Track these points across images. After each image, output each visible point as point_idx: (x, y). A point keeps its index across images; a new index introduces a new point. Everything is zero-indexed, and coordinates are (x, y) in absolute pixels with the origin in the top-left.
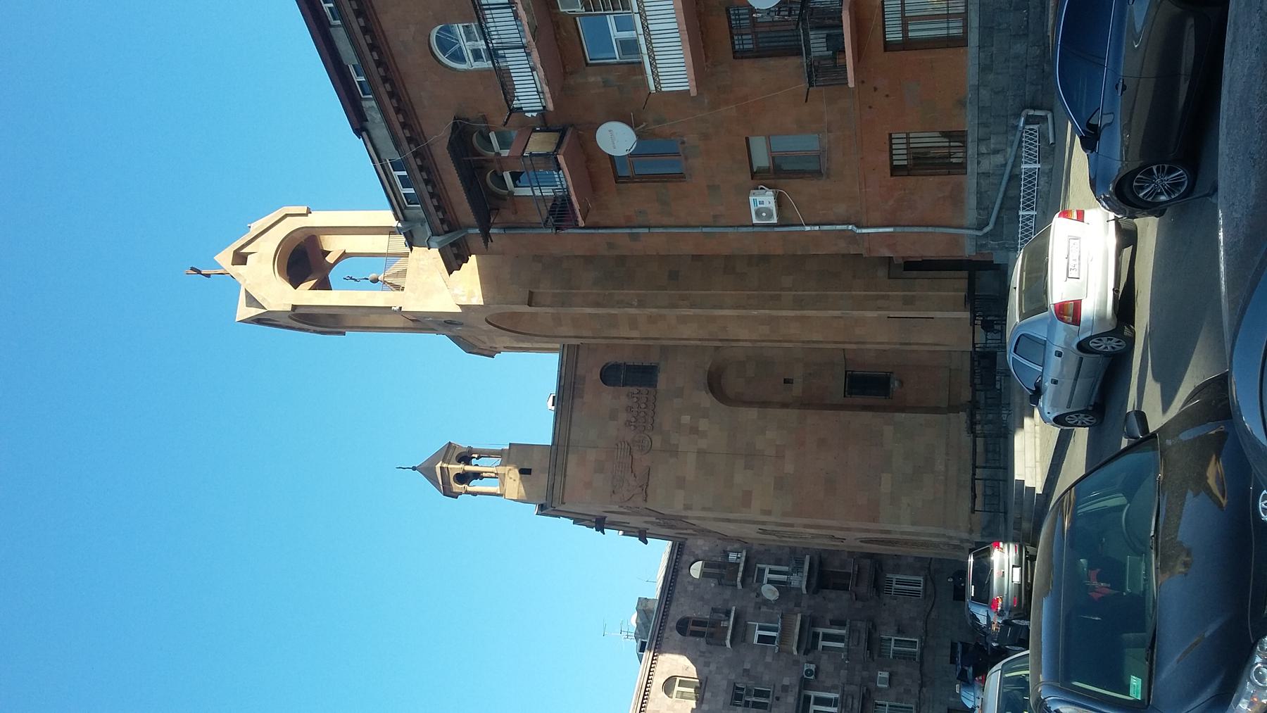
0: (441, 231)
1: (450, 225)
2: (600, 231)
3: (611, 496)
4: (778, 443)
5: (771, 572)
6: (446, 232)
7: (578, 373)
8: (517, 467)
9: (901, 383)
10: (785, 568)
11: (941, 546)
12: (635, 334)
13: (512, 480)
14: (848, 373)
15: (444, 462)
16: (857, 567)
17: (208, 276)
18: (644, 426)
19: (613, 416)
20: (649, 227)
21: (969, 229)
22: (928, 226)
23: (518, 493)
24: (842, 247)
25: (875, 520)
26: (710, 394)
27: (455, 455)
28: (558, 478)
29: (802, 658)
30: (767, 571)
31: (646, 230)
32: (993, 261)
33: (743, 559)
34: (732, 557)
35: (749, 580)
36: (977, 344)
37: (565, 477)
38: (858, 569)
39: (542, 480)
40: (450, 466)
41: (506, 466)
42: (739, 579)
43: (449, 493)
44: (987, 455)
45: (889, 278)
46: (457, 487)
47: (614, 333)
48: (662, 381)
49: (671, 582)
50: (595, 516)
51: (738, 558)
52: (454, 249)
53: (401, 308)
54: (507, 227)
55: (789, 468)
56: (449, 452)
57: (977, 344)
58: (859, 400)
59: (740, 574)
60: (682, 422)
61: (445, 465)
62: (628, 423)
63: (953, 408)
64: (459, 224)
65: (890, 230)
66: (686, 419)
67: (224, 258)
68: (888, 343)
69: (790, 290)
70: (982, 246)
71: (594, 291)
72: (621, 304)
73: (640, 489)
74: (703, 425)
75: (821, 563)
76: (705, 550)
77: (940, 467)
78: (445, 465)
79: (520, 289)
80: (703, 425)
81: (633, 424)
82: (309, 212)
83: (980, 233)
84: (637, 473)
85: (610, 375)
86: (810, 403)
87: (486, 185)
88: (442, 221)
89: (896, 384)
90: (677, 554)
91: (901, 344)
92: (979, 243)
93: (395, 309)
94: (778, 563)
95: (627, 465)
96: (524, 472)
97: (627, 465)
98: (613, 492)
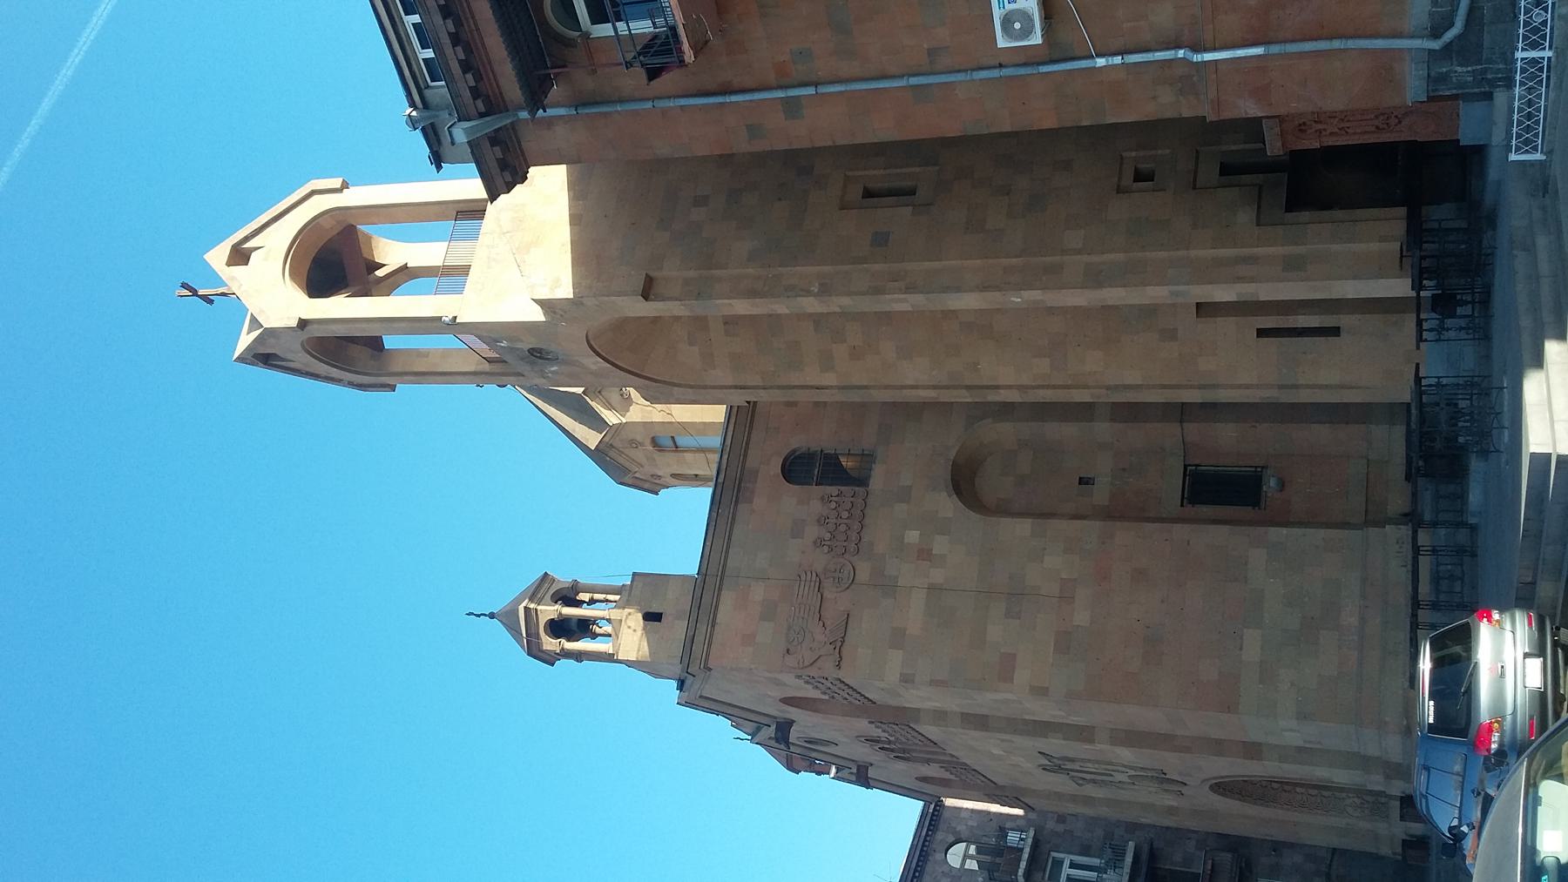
0: (473, 112)
1: (488, 101)
2: (734, 98)
4: (1064, 576)
5: (1073, 865)
6: (482, 115)
7: (748, 464)
8: (640, 611)
9: (1282, 485)
10: (1096, 861)
11: (1350, 810)
12: (830, 379)
13: (631, 631)
14: (1189, 468)
15: (531, 600)
16: (1210, 862)
17: (207, 299)
19: (797, 531)
20: (816, 85)
21: (1412, 37)
22: (1331, 38)
23: (639, 650)
24: (1165, 104)
25: (1230, 707)
28: (702, 628)
30: (1067, 863)
31: (811, 91)
32: (1458, 141)
33: (1030, 841)
34: (1013, 837)
35: (1037, 876)
36: (1424, 378)
37: (713, 626)
38: (1213, 866)
39: (676, 629)
40: (539, 608)
41: (624, 608)
42: (1021, 872)
43: (534, 651)
45: (1258, 225)
46: (550, 644)
47: (795, 378)
48: (878, 479)
49: (915, 871)
50: (775, 718)
51: (1021, 839)
52: (497, 149)
53: (456, 317)
54: (581, 101)
55: (1081, 618)
56: (543, 587)
58: (1206, 510)
59: (1023, 865)
60: (906, 541)
61: (532, 606)
62: (819, 543)
63: (1373, 518)
65: (1258, 51)
66: (913, 536)
67: (217, 257)
68: (1258, 386)
69: (1079, 252)
70: (1443, 79)
71: (750, 270)
72: (793, 291)
74: (940, 545)
75: (1153, 855)
76: (972, 826)
78: (532, 606)
79: (633, 272)
80: (940, 545)
81: (829, 543)
82: (345, 185)
83: (1435, 45)
84: (828, 623)
85: (797, 469)
86: (1122, 511)
87: (544, 22)
88: (476, 93)
89: (1273, 482)
90: (928, 830)
91: (1281, 387)
92: (1433, 74)
93: (447, 319)
94: (1085, 851)
96: (651, 617)
97: (812, 608)
98: (788, 650)
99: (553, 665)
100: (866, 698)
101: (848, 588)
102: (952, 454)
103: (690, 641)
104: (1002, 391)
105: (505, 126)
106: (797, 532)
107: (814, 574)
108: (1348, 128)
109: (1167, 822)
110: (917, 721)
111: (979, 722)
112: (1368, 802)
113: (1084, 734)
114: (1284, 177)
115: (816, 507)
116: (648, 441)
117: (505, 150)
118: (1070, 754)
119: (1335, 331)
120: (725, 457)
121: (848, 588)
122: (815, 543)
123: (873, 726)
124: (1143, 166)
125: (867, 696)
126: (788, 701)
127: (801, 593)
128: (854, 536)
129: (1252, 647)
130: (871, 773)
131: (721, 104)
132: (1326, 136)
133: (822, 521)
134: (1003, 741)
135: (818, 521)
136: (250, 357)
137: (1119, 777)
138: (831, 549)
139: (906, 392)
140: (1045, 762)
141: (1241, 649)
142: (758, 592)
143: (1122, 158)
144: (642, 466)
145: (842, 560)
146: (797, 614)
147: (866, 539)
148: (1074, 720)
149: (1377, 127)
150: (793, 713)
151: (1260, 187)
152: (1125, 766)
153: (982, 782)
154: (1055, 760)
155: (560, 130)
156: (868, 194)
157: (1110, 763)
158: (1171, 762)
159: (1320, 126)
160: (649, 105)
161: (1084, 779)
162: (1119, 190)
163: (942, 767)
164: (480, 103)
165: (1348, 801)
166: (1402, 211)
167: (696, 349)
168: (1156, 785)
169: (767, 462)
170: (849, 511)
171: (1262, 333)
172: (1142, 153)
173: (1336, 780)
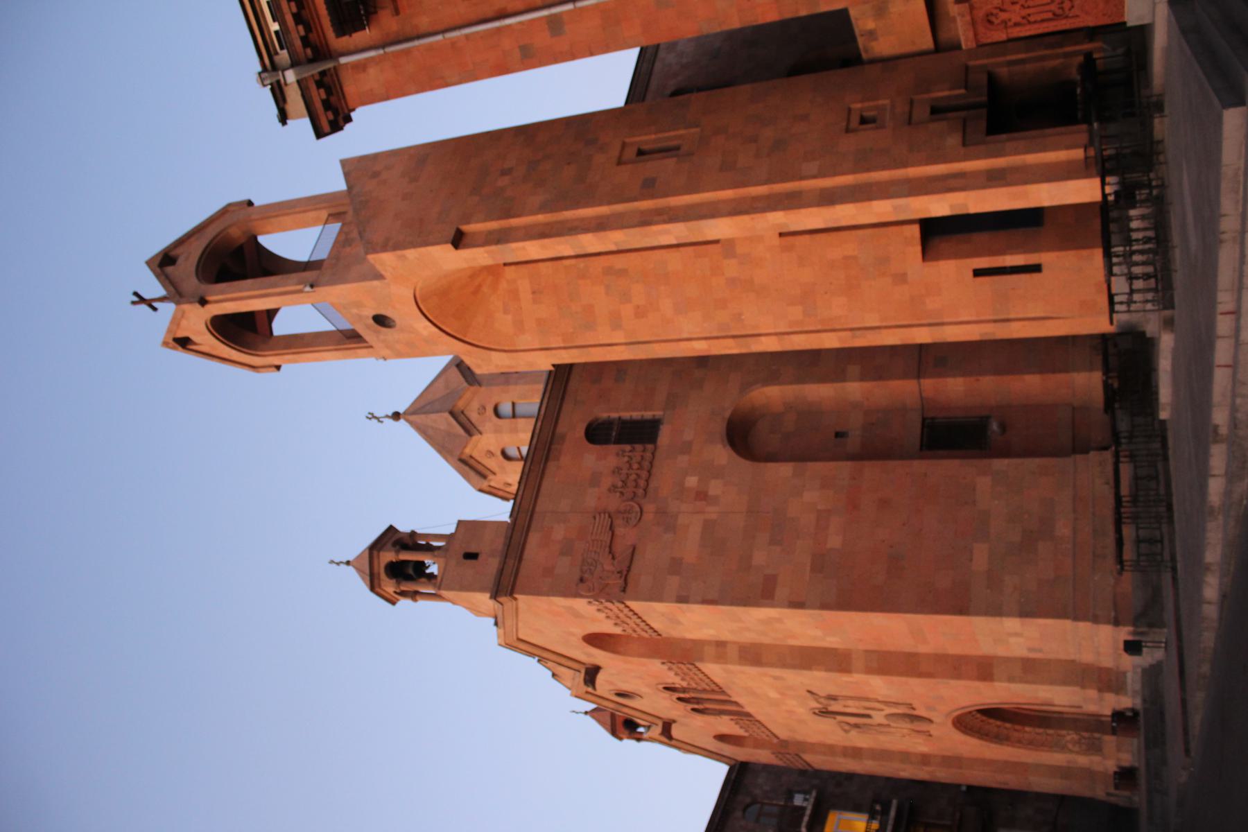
3: (577, 585)
6: (311, 61)
9: (1003, 427)
11: (1070, 746)
12: (619, 337)
14: (927, 421)
19: (595, 480)
26: (728, 447)
27: (394, 539)
28: (511, 562)
32: (1125, 23)
33: (812, 800)
36: (1117, 294)
44: (1138, 547)
57: (1117, 294)
59: (806, 819)
62: (613, 489)
63: (1079, 447)
64: (329, 51)
73: (619, 575)
74: (715, 488)
77: (1063, 529)
81: (620, 490)
84: (617, 555)
85: (597, 433)
88: (305, 41)
97: (604, 543)
99: (393, 603)
100: (651, 628)
101: (635, 526)
102: (727, 414)
103: (501, 572)
104: (763, 339)
105: (329, 69)
106: (595, 480)
107: (607, 515)
108: (1029, 15)
109: (922, 774)
110: (702, 660)
111: (753, 655)
112: (1084, 738)
113: (838, 661)
114: (984, 112)
116: (499, 453)
117: (329, 92)
118: (833, 690)
119: (1036, 268)
120: (539, 424)
121: (635, 526)
122: (609, 490)
123: (665, 667)
124: (866, 114)
125: (649, 622)
126: (595, 640)
128: (642, 483)
129: (981, 557)
130: (676, 731)
131: (499, 30)
132: (1011, 27)
134: (776, 678)
135: (614, 472)
136: (171, 341)
137: (878, 718)
138: (622, 493)
139: (683, 345)
140: (815, 705)
141: (971, 560)
142: (559, 533)
143: (850, 110)
144: (494, 474)
147: (653, 484)
148: (832, 641)
149: (1054, 14)
150: (597, 656)
151: (965, 121)
152: (879, 702)
153: (768, 736)
155: (372, 71)
156: (641, 153)
157: (867, 699)
158: (915, 690)
159: (1003, 16)
160: (440, 37)
161: (848, 724)
162: (848, 130)
163: (732, 720)
164: (309, 51)
165: (1068, 738)
166: (1084, 127)
167: (509, 317)
168: (909, 726)
169: (573, 425)
170: (639, 463)
171: (978, 273)
172: (866, 104)
173: (1056, 702)
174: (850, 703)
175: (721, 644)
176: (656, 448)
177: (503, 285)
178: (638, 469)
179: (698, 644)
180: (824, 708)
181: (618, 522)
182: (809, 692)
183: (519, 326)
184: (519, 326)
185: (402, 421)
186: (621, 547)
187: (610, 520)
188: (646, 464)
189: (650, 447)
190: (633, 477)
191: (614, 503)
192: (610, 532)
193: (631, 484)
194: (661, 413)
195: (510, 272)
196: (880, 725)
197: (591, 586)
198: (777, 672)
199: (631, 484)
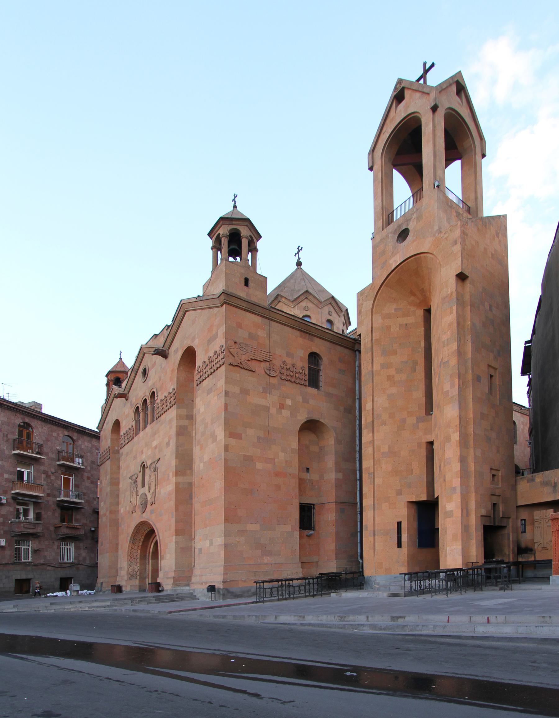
18: (284, 374)
29: (10, 496)
62: (284, 363)
81: (285, 367)
84: (249, 363)
95: (256, 356)
97: (256, 356)
107: (272, 359)
115: (299, 364)
122: (285, 361)
127: (263, 352)
133: (294, 365)
145: (278, 372)
146: (253, 349)
154: (154, 465)
170: (299, 377)
174: (153, 477)
175: (191, 417)
176: (306, 386)
177: (412, 309)
178: (296, 377)
179: (191, 404)
180: (147, 466)
181: (267, 364)
182: (160, 459)
183: (387, 316)
184: (387, 316)
185: (296, 267)
186: (254, 365)
187: (268, 360)
188: (298, 381)
189: (307, 384)
190: (291, 374)
191: (278, 363)
192: (262, 360)
193: (288, 373)
194: (322, 390)
195: (420, 313)
196: (138, 491)
197: (233, 347)
198: (173, 443)
199: (288, 373)
